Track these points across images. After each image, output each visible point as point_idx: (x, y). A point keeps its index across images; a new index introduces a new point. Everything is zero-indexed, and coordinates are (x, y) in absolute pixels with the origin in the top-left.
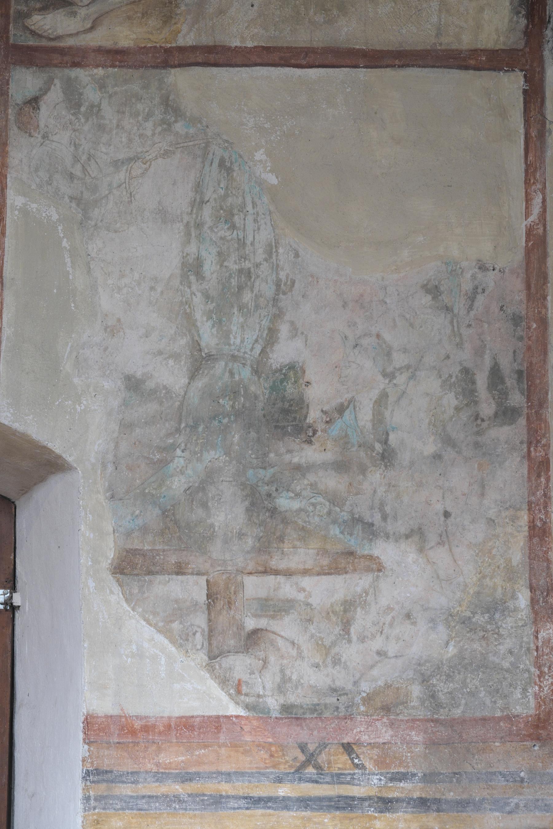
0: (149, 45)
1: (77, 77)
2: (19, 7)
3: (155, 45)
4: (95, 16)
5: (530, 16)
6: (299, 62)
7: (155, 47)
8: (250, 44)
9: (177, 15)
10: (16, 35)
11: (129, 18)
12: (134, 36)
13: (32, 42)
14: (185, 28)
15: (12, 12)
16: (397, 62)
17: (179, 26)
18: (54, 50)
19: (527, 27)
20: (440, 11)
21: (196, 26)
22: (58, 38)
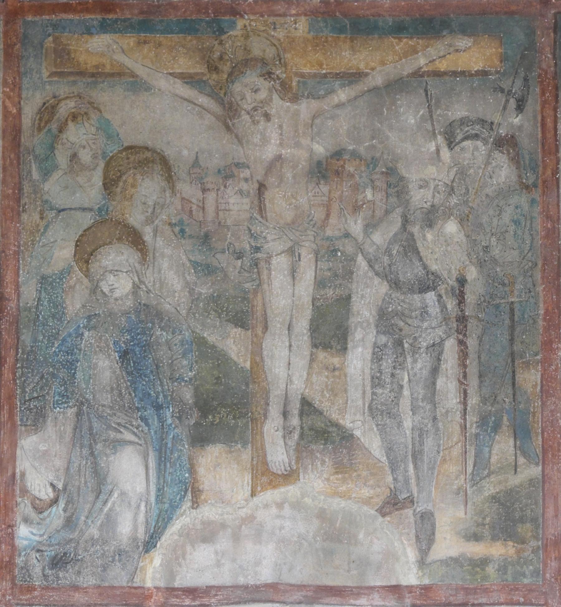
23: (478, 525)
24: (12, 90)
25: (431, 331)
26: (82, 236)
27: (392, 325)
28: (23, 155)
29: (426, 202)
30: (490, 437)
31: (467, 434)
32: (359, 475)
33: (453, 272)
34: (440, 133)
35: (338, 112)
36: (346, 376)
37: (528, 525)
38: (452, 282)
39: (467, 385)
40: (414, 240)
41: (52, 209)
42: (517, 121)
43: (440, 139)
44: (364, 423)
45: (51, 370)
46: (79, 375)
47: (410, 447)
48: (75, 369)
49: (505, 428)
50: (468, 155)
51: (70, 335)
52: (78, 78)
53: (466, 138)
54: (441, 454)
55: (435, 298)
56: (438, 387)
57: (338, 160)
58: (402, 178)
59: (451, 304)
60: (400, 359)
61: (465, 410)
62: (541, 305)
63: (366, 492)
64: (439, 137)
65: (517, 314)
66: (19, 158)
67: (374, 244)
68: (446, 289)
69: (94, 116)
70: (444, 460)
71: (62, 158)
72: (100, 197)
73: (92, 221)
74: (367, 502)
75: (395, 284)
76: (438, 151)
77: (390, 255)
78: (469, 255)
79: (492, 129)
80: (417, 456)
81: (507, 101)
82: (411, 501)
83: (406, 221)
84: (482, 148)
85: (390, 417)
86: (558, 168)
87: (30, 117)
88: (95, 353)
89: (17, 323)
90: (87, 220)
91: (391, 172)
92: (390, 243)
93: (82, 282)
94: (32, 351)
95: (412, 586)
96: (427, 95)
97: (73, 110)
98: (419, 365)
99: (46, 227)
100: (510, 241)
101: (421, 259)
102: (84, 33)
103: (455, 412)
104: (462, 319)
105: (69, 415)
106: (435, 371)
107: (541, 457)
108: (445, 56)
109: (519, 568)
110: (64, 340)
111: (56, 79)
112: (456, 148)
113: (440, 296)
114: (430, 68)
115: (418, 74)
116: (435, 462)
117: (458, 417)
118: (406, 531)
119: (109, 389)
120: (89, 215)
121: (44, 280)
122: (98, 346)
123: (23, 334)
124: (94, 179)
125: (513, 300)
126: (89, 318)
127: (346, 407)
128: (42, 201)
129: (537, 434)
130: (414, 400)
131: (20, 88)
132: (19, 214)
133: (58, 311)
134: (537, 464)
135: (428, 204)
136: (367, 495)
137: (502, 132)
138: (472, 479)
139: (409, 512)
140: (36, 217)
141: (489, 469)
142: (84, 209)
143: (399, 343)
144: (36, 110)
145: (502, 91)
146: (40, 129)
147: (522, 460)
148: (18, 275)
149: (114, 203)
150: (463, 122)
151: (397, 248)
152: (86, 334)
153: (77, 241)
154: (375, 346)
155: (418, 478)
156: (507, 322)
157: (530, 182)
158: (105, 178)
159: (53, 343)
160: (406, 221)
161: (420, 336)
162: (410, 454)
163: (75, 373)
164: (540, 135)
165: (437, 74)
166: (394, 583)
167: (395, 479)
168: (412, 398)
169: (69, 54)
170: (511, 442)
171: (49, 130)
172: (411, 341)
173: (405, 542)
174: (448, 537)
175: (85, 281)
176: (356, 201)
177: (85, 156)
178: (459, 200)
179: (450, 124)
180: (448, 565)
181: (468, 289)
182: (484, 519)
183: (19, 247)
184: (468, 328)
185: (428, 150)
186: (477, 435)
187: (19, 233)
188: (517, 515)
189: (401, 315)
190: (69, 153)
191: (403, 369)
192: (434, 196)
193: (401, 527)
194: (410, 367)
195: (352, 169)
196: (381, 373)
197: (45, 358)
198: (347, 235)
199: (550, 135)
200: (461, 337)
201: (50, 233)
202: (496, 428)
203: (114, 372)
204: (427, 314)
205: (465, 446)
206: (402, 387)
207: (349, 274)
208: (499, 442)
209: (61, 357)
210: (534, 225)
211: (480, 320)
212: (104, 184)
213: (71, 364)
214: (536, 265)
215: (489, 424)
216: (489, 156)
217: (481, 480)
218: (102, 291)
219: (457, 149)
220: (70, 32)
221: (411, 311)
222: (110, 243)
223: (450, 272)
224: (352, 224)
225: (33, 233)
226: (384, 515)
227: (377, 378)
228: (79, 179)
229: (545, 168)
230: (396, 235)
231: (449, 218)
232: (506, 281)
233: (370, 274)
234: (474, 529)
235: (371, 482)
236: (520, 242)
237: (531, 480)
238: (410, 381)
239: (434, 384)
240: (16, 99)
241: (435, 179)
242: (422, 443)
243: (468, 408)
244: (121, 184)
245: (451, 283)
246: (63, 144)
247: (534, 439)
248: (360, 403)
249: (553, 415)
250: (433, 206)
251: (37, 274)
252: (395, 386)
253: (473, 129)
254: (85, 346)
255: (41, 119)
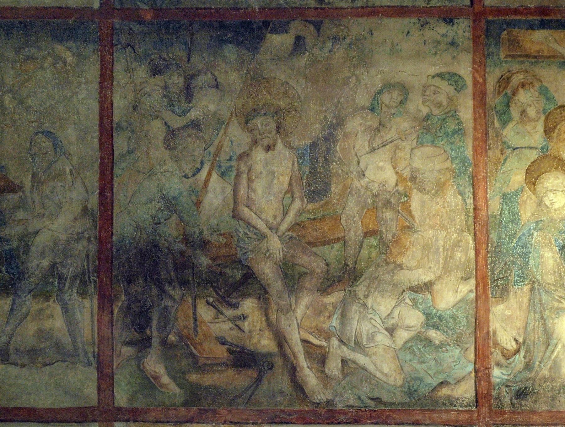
24: (479, 66)
26: (530, 166)
28: (488, 111)
41: (509, 147)
45: (512, 259)
46: (531, 262)
48: (528, 258)
51: (524, 235)
52: (525, 59)
66: (485, 113)
69: (537, 85)
71: (515, 113)
72: (542, 139)
73: (537, 156)
87: (492, 84)
88: (542, 247)
89: (487, 226)
90: (534, 155)
93: (531, 199)
94: (498, 246)
97: (522, 81)
99: (505, 160)
102: (528, 29)
105: (525, 290)
110: (520, 238)
111: (510, 59)
119: (552, 272)
120: (535, 152)
121: (504, 196)
122: (544, 243)
123: (491, 233)
124: (538, 127)
126: (537, 223)
128: (502, 142)
131: (485, 66)
132: (486, 152)
133: (515, 219)
140: (498, 152)
142: (531, 148)
144: (496, 80)
146: (499, 93)
148: (486, 192)
149: (552, 144)
152: (535, 234)
153: (527, 170)
158: (545, 127)
159: (513, 240)
163: (528, 261)
169: (518, 42)
171: (506, 94)
175: (534, 197)
177: (532, 112)
183: (486, 173)
187: (486, 164)
190: (521, 109)
197: (507, 251)
201: (508, 164)
203: (556, 261)
209: (519, 250)
212: (545, 131)
213: (525, 254)
218: (545, 204)
220: (519, 28)
222: (550, 171)
225: (496, 164)
228: (527, 127)
240: (483, 73)
244: (556, 131)
246: (515, 103)
251: (500, 193)
254: (535, 242)
255: (500, 87)
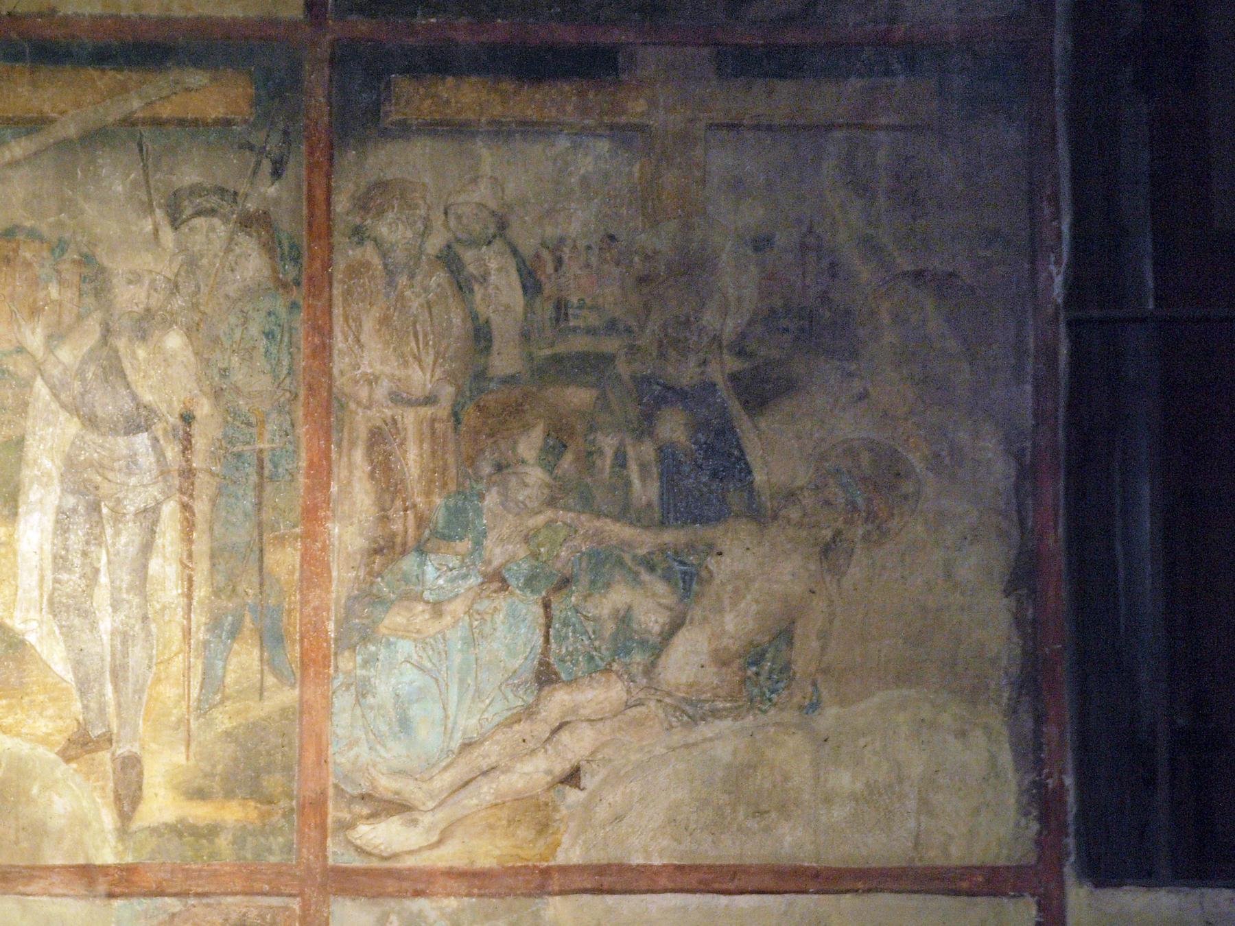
0: (519, 864)
1: (421, 911)
2: (340, 814)
3: (525, 863)
4: (442, 826)
5: (1043, 818)
6: (725, 886)
7: (526, 867)
8: (657, 862)
9: (555, 821)
10: (338, 855)
11: (491, 827)
12: (497, 852)
13: (358, 862)
14: (566, 840)
15: (330, 820)
16: (860, 885)
17: (559, 836)
18: (390, 873)
19: (1040, 833)
20: (919, 813)
21: (583, 837)
22: (394, 856)
23: (206, 776)
25: (141, 489)
27: (84, 481)
29: (137, 304)
30: (225, 644)
31: (192, 641)
32: (32, 701)
33: (176, 403)
34: (160, 206)
35: (10, 173)
36: (15, 553)
37: (278, 776)
38: (174, 420)
39: (193, 570)
40: (118, 358)
42: (272, 191)
43: (159, 214)
44: (41, 623)
47: (109, 659)
49: (246, 632)
50: (200, 238)
53: (199, 213)
54: (154, 669)
55: (148, 443)
56: (151, 572)
57: (9, 241)
58: (102, 270)
59: (172, 452)
60: (97, 531)
61: (190, 605)
62: (303, 455)
63: (42, 726)
64: (158, 211)
65: (268, 466)
67: (59, 362)
68: (165, 429)
70: (158, 680)
74: (45, 741)
75: (90, 420)
76: (156, 231)
77: (83, 380)
78: (199, 380)
79: (235, 201)
80: (118, 673)
81: (258, 164)
82: (108, 739)
83: (107, 332)
84: (222, 229)
85: (79, 616)
86: (330, 259)
91: (87, 260)
92: (84, 362)
95: (108, 867)
96: (141, 150)
98: (123, 539)
100: (260, 362)
101: (128, 386)
103: (175, 609)
104: (188, 473)
106: (147, 548)
107: (298, 675)
108: (168, 97)
109: (262, 840)
112: (182, 227)
113: (156, 440)
114: (148, 114)
115: (129, 122)
116: (145, 681)
117: (180, 612)
118: (100, 783)
125: (262, 446)
127: (15, 601)
129: (294, 641)
130: (115, 590)
134: (293, 686)
135: (141, 306)
136: (44, 730)
137: (251, 206)
138: (198, 708)
139: (105, 756)
141: (223, 692)
143: (95, 507)
145: (251, 148)
147: (270, 680)
150: (194, 190)
151: (93, 368)
154: (60, 510)
155: (119, 705)
156: (254, 478)
157: (290, 278)
160: (108, 331)
161: (125, 498)
162: (107, 669)
164: (305, 212)
165: (157, 122)
166: (81, 861)
167: (86, 707)
168: (113, 587)
170: (256, 653)
172: (111, 504)
173: (98, 800)
174: (162, 792)
176: (35, 301)
178: (184, 301)
179: (175, 194)
180: (161, 835)
181: (196, 429)
182: (214, 766)
184: (197, 484)
185: (141, 230)
186: (206, 644)
188: (262, 762)
189: (100, 467)
191: (100, 545)
192: (149, 296)
193: (93, 778)
194: (110, 542)
195: (28, 255)
196: (67, 550)
198: (21, 350)
199: (320, 213)
200: (185, 499)
202: (234, 634)
204: (136, 464)
205: (189, 657)
206: (97, 571)
207: (23, 407)
208: (238, 654)
210: (294, 340)
211: (212, 474)
214: (297, 395)
215: (226, 629)
216: (232, 239)
217: (210, 709)
219: (185, 229)
221: (114, 460)
223: (170, 405)
224: (28, 332)
226: (68, 760)
227: (61, 557)
229: (312, 258)
230: (92, 350)
231: (171, 326)
232: (253, 420)
233: (54, 406)
234: (199, 782)
235: (50, 712)
236: (273, 362)
237: (283, 710)
238: (109, 562)
239: (145, 566)
241: (151, 272)
242: (125, 655)
243: (195, 603)
245: (171, 420)
247: (289, 649)
248: (36, 594)
249: (316, 615)
250: (148, 310)
252: (88, 570)
253: (207, 201)
